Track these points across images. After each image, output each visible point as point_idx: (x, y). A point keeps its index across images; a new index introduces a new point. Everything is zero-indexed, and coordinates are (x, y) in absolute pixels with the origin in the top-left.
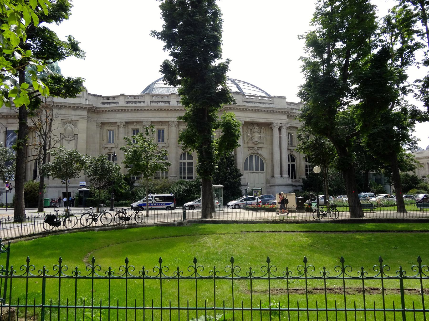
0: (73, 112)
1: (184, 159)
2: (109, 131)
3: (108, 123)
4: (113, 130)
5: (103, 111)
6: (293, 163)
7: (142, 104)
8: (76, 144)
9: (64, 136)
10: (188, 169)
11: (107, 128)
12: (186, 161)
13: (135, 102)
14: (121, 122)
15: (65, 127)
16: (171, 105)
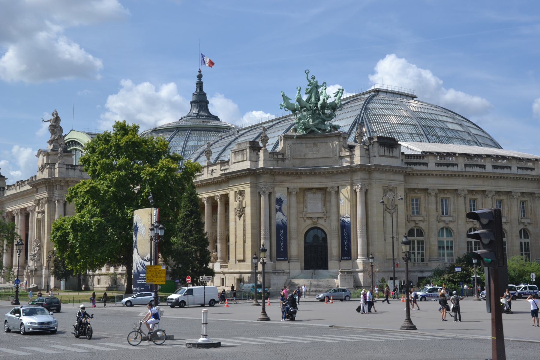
0: (392, 177)
3: (414, 190)
4: (418, 199)
6: (526, 240)
7: (455, 168)
9: (386, 207)
10: (418, 248)
11: (412, 195)
14: (434, 190)
16: (486, 171)
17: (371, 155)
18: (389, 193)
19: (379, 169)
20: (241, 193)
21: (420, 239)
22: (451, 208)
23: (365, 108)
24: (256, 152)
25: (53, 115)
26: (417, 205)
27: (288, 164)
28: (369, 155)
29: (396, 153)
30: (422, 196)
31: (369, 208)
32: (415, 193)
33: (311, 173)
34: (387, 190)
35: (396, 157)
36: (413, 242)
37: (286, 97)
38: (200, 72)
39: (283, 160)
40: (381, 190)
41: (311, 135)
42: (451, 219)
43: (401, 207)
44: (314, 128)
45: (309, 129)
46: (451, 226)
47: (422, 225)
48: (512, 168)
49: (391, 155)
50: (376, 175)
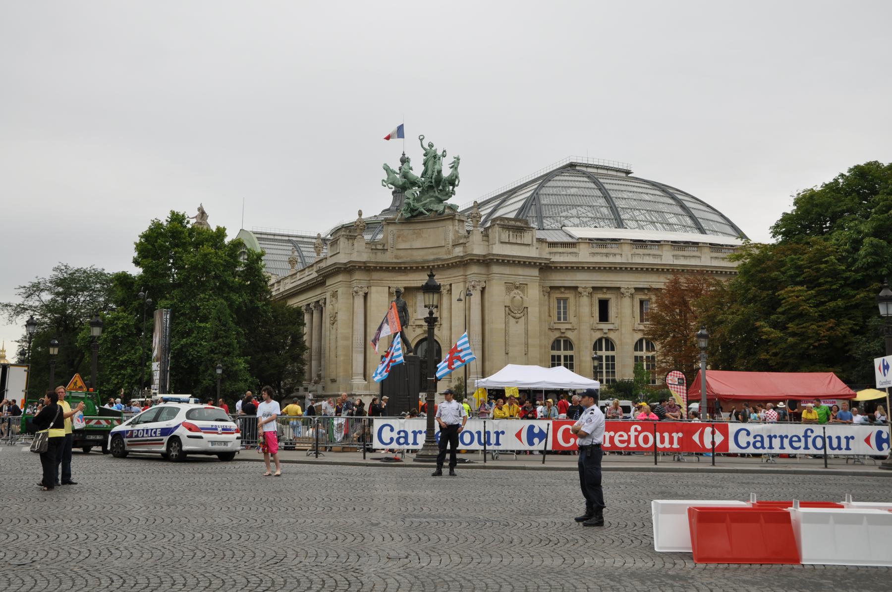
0: (520, 271)
1: (641, 350)
2: (559, 300)
4: (565, 300)
5: (556, 267)
8: (527, 323)
12: (644, 353)
13: (607, 255)
14: (585, 288)
15: (512, 294)
17: (491, 242)
18: (516, 291)
20: (335, 295)
21: (569, 353)
22: (612, 311)
23: (541, 186)
24: (350, 242)
25: (199, 209)
26: (565, 308)
27: (388, 258)
28: (488, 241)
30: (570, 295)
31: (486, 312)
32: (562, 293)
34: (512, 287)
36: (559, 357)
38: (404, 154)
39: (384, 250)
40: (503, 288)
41: (421, 217)
42: (611, 327)
43: (534, 311)
44: (422, 210)
46: (612, 336)
47: (570, 335)
48: (703, 259)
50: (496, 269)
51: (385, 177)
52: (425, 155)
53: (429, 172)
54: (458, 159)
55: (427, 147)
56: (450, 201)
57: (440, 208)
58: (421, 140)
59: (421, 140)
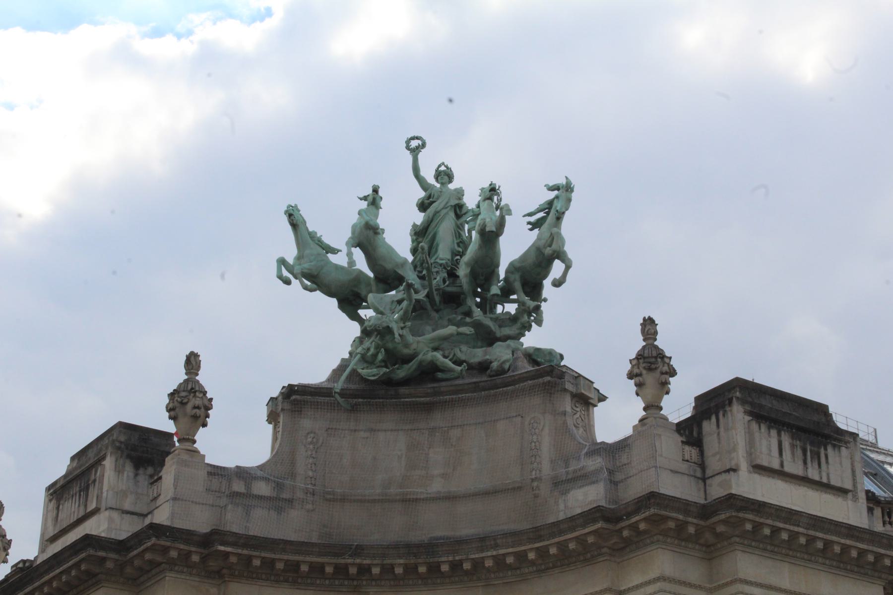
17: (714, 464)
19: (758, 526)
28: (702, 466)
29: (837, 467)
33: (410, 570)
35: (842, 491)
37: (312, 236)
45: (407, 360)
49: (813, 474)
50: (747, 565)
51: (291, 253)
52: (423, 206)
53: (443, 253)
54: (568, 188)
55: (431, 180)
56: (532, 339)
57: (500, 353)
58: (415, 152)
59: (415, 152)
